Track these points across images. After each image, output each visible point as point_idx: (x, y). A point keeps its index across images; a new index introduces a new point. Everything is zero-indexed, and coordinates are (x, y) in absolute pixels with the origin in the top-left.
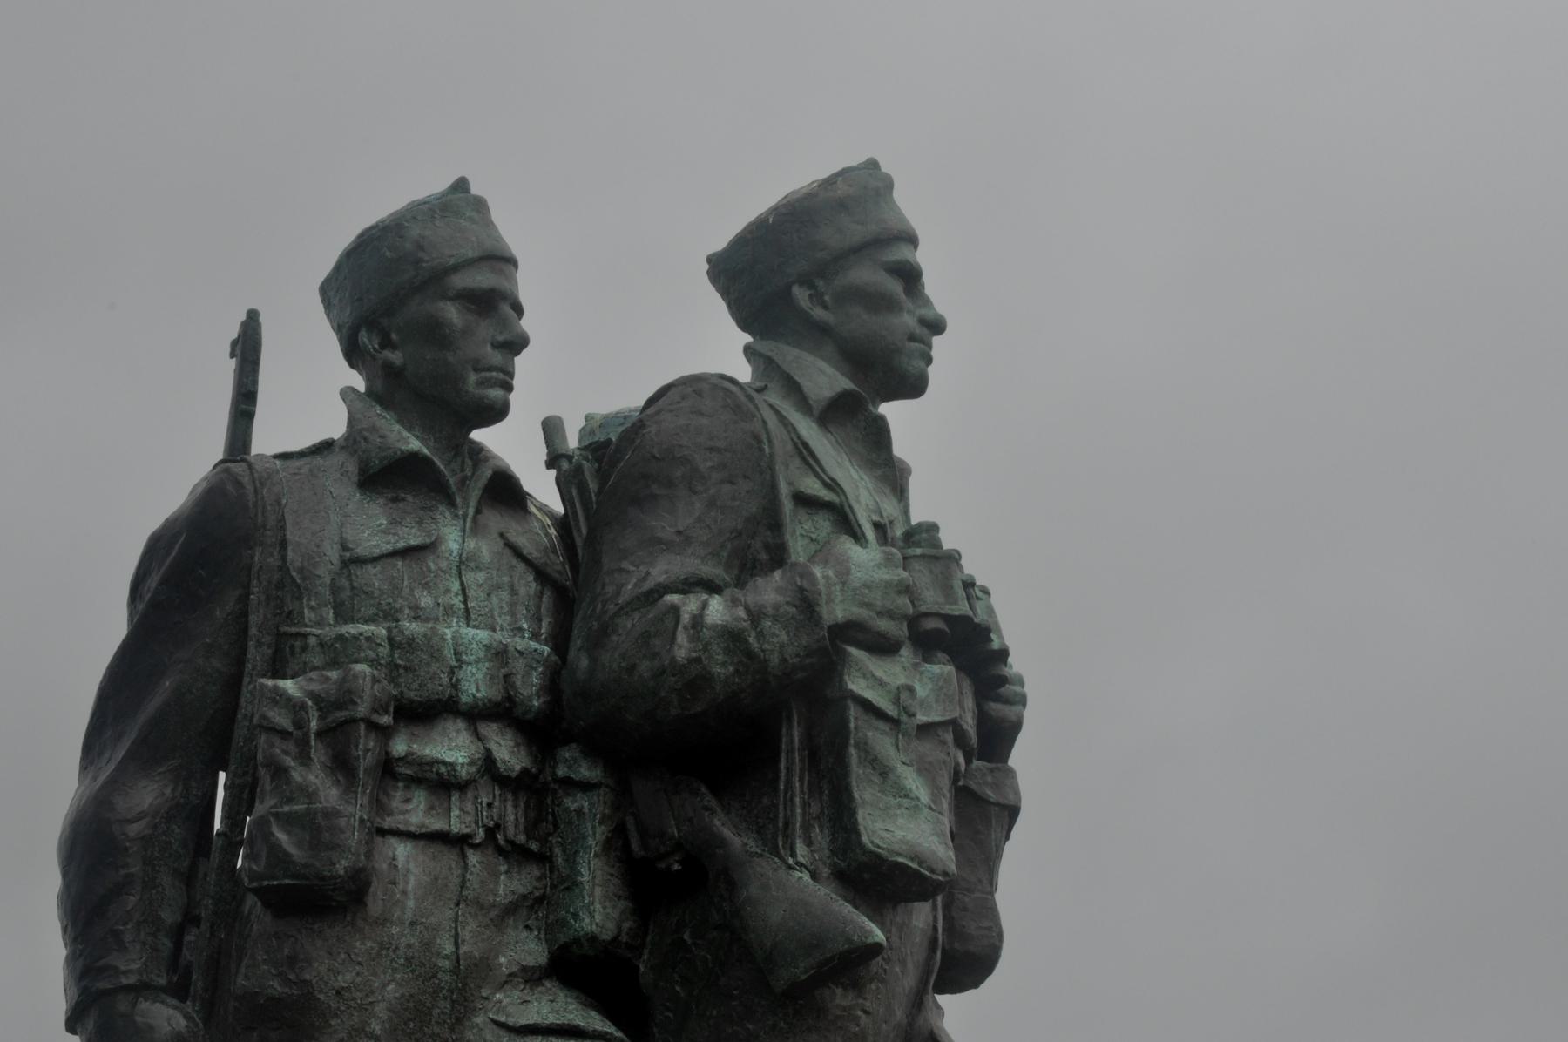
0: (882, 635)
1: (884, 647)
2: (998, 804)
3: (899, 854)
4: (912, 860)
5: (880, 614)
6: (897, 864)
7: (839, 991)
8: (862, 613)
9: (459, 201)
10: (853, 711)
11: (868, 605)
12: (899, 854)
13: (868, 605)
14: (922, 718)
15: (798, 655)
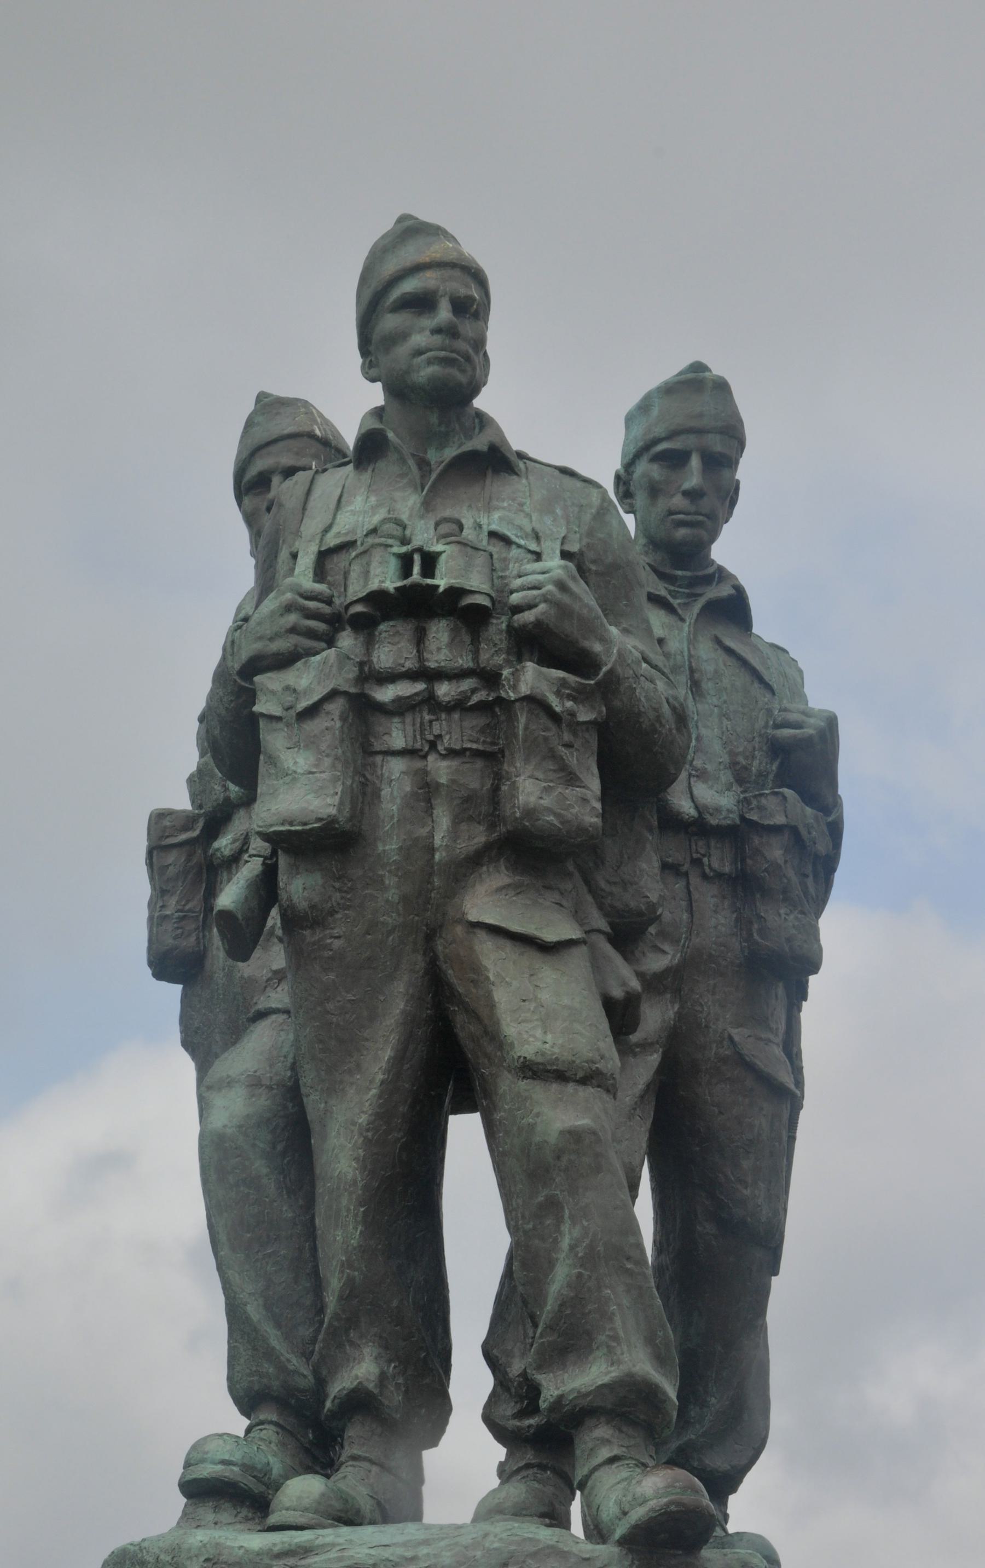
0: (276, 654)
1: (284, 661)
2: (516, 700)
3: (271, 826)
4: (283, 824)
5: (271, 639)
6: (275, 832)
7: (307, 933)
8: (257, 647)
9: (268, 405)
10: (262, 723)
11: (260, 638)
12: (271, 826)
13: (260, 638)
14: (303, 704)
15: (231, 701)
